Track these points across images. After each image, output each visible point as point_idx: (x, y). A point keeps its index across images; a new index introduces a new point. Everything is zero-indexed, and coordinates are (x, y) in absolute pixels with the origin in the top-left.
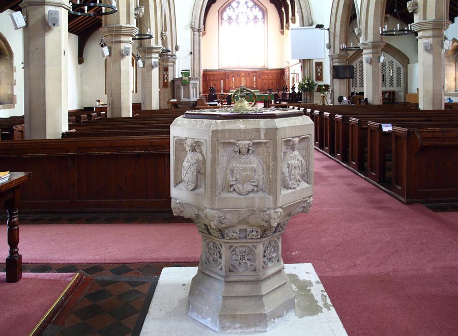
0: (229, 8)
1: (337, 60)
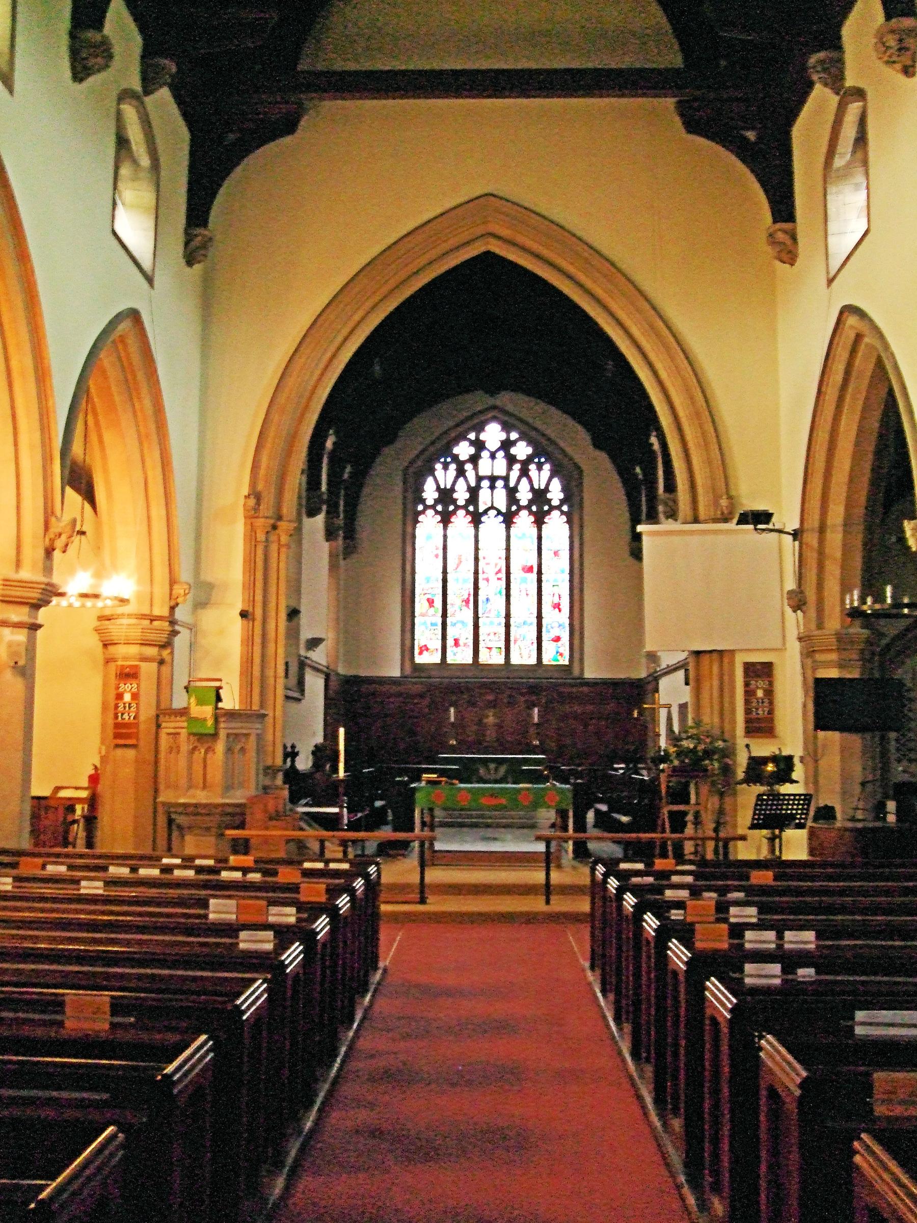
0: (446, 467)
1: (834, 656)
